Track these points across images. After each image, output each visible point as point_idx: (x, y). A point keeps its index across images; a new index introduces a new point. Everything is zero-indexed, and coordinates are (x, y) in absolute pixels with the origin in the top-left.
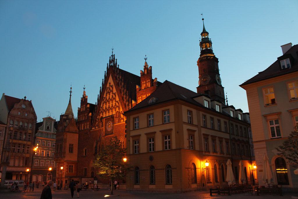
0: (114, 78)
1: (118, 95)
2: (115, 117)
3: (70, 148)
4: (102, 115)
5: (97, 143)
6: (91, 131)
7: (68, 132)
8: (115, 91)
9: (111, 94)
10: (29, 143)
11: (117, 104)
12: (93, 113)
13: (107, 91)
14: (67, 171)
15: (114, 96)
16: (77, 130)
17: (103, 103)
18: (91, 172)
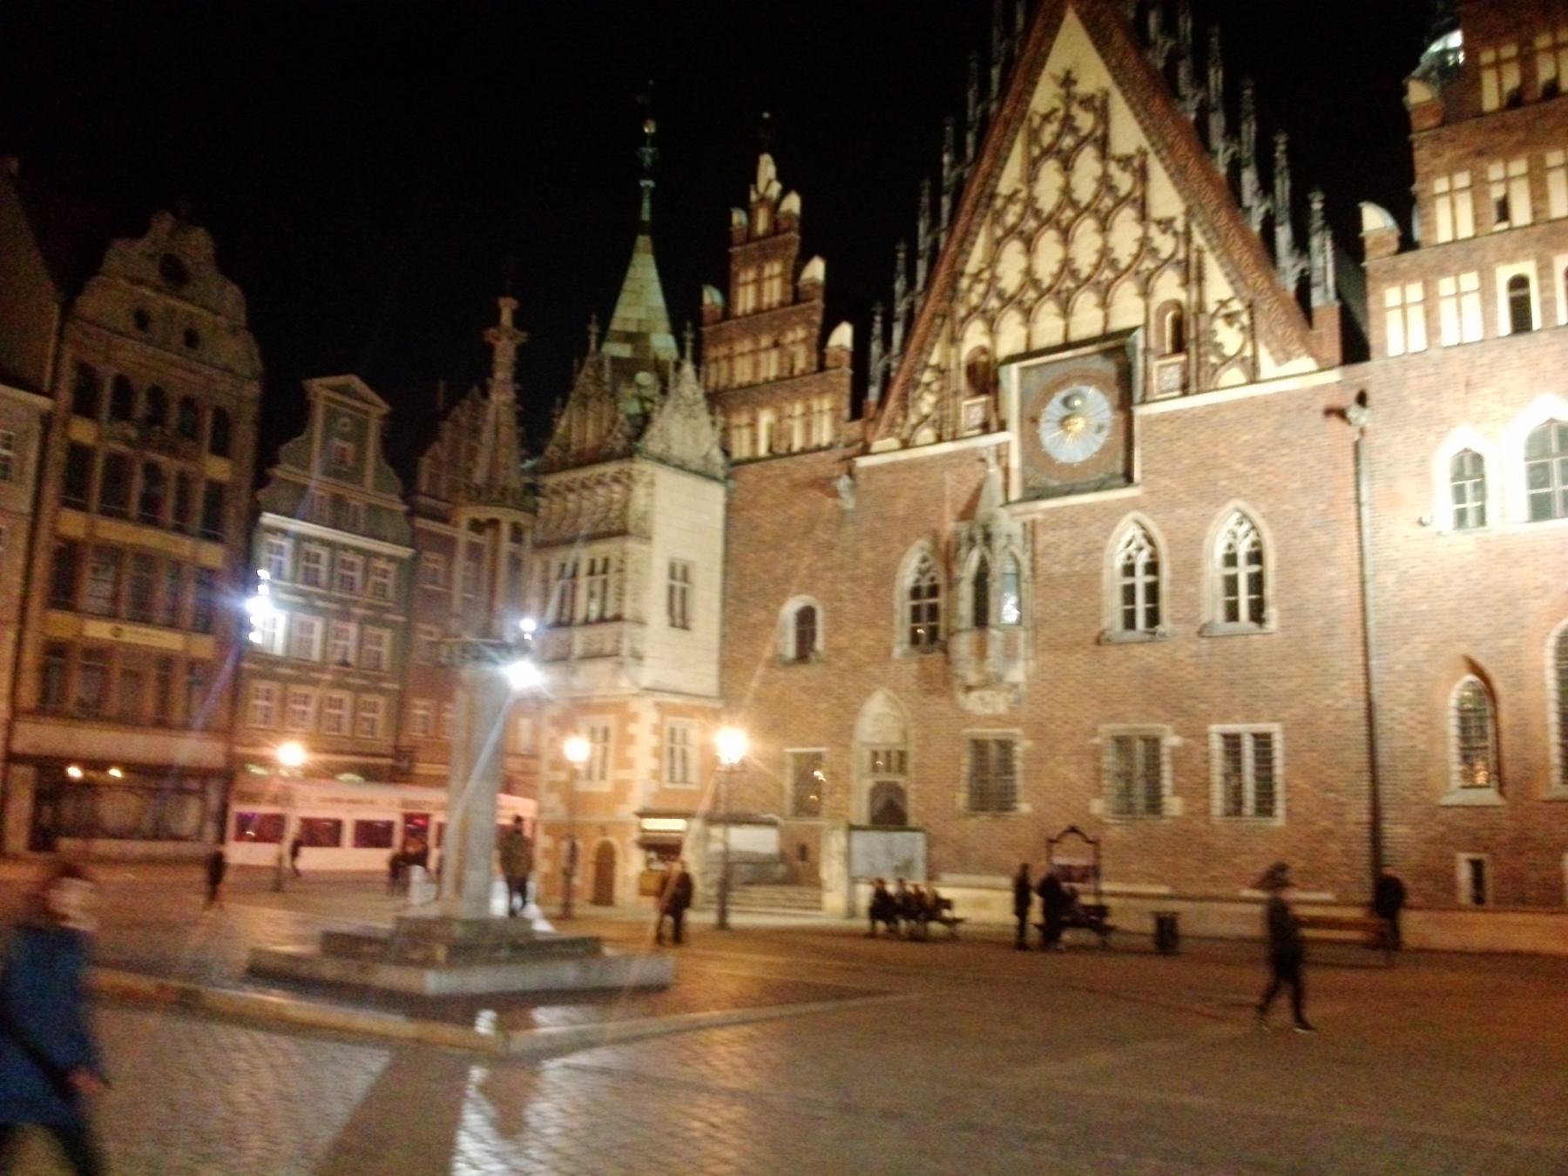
0: (1118, 39)
1: (1178, 175)
2: (1146, 350)
3: (671, 589)
4: (985, 341)
5: (947, 555)
6: (863, 462)
7: (662, 460)
8: (1127, 133)
9: (1088, 165)
10: (212, 555)
11: (1165, 244)
12: (877, 329)
13: (1034, 136)
14: (656, 775)
15: (1124, 182)
16: (717, 455)
17: (998, 243)
18: (868, 783)
